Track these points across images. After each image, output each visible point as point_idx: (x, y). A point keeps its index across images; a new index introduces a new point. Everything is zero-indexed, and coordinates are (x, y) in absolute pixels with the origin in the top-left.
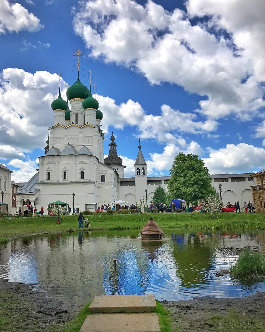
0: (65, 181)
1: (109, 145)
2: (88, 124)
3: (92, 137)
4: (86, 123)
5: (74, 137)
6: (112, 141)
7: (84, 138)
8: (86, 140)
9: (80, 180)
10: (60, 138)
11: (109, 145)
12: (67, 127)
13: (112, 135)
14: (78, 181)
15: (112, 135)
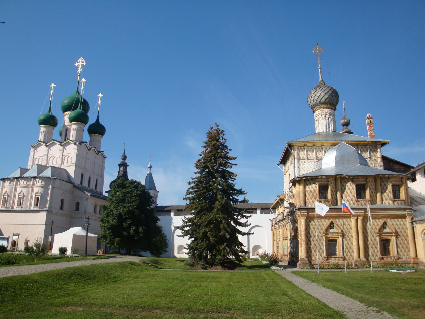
0: (19, 209)
1: (119, 165)
2: (69, 141)
3: (71, 156)
4: (66, 140)
5: (53, 157)
6: (122, 159)
7: (64, 156)
8: (66, 159)
9: (34, 208)
10: (40, 157)
11: (119, 165)
12: (47, 145)
13: (124, 153)
14: (32, 209)
15: (124, 153)
